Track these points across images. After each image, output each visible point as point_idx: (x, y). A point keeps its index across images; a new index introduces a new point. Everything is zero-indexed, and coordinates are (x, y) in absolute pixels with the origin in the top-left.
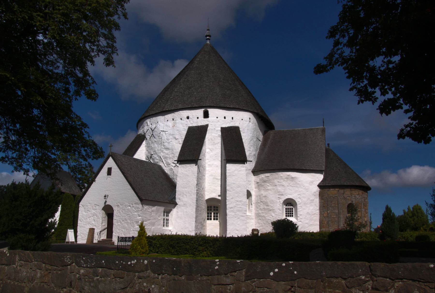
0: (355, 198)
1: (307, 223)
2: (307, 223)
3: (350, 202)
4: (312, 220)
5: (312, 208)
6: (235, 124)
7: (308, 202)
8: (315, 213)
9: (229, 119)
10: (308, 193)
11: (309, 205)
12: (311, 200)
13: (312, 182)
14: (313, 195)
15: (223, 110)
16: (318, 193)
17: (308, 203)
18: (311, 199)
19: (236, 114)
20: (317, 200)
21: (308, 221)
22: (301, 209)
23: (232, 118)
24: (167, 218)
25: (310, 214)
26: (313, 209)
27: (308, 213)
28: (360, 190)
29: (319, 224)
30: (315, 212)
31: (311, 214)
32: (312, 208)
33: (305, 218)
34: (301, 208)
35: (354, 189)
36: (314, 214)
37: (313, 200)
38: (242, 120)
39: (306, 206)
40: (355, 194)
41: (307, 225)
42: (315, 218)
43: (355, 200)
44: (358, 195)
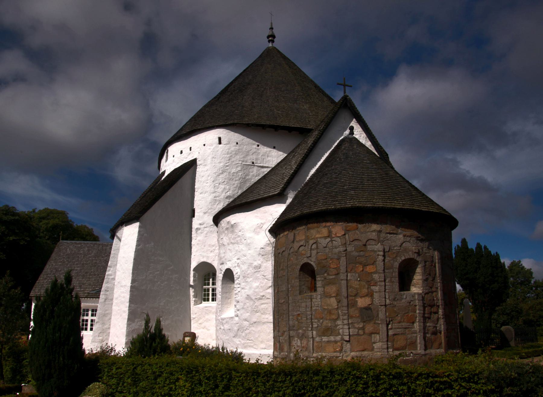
0: (317, 248)
1: (246, 320)
2: (246, 320)
3: (305, 260)
4: (257, 312)
5: (255, 284)
6: (193, 157)
7: (249, 272)
8: (263, 296)
9: (186, 151)
10: (249, 252)
11: (251, 279)
12: (256, 267)
13: (260, 227)
14: (260, 254)
15: (180, 141)
16: (270, 249)
17: (248, 274)
18: (255, 264)
19: (196, 141)
20: (269, 266)
21: (248, 314)
22: (239, 289)
23: (191, 148)
24: (93, 318)
25: (252, 299)
26: (258, 287)
27: (248, 297)
28: (337, 221)
29: (272, 321)
30: (262, 294)
31: (253, 298)
32: (255, 284)
33: (243, 308)
34: (239, 286)
35: (315, 225)
36: (260, 299)
37: (259, 267)
38: (204, 145)
39: (247, 282)
40: (317, 236)
41: (246, 323)
42: (263, 306)
43: (317, 253)
44: (325, 238)
